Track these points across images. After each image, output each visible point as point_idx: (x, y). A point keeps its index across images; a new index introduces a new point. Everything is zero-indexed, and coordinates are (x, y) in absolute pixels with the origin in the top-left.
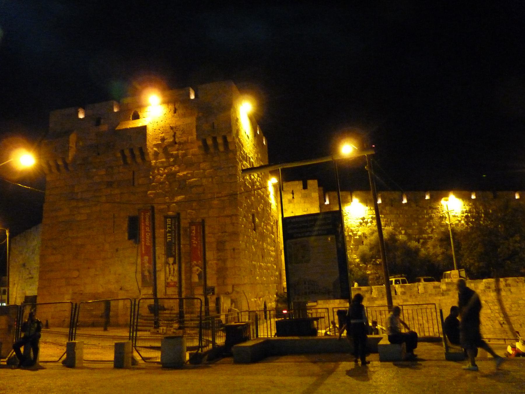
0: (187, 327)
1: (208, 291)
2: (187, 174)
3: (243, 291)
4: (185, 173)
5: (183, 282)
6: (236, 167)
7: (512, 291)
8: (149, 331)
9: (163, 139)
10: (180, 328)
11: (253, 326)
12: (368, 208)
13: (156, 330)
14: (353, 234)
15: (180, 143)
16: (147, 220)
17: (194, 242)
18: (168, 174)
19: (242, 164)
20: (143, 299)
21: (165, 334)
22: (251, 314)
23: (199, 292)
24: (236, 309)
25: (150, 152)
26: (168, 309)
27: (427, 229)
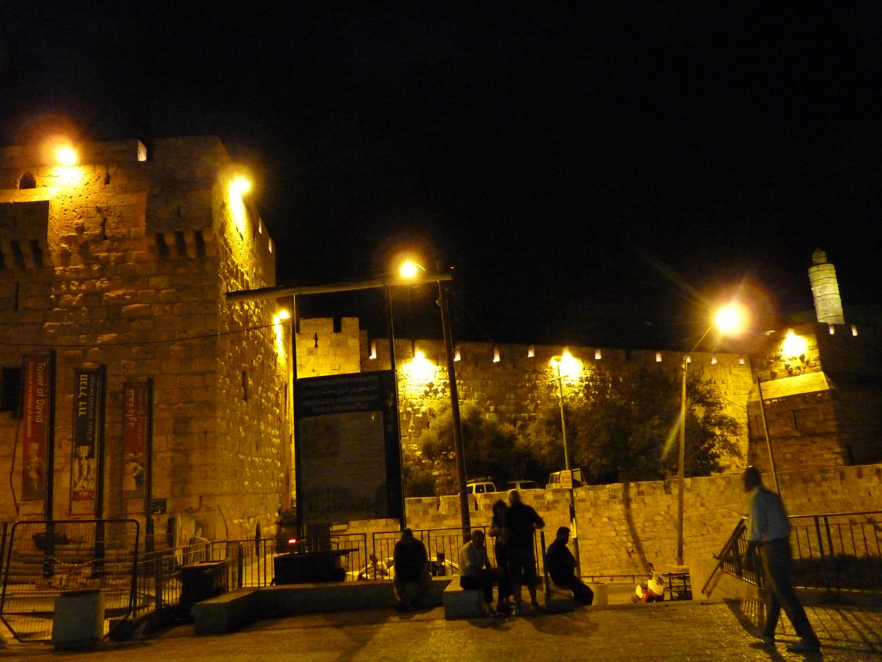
0: (110, 573)
1: (153, 506)
2: (124, 294)
3: (219, 506)
4: (120, 292)
5: (106, 490)
6: (215, 287)
7: (646, 501)
8: (33, 583)
9: (80, 229)
10: (94, 576)
11: (233, 566)
12: (439, 368)
13: (46, 582)
14: (413, 409)
15: (113, 239)
16: (40, 375)
17: (132, 419)
18: (86, 294)
19: (228, 284)
20: (20, 522)
21: (64, 588)
22: (231, 547)
23: (135, 509)
24: (203, 539)
25: (54, 251)
26: (74, 542)
27: (528, 405)
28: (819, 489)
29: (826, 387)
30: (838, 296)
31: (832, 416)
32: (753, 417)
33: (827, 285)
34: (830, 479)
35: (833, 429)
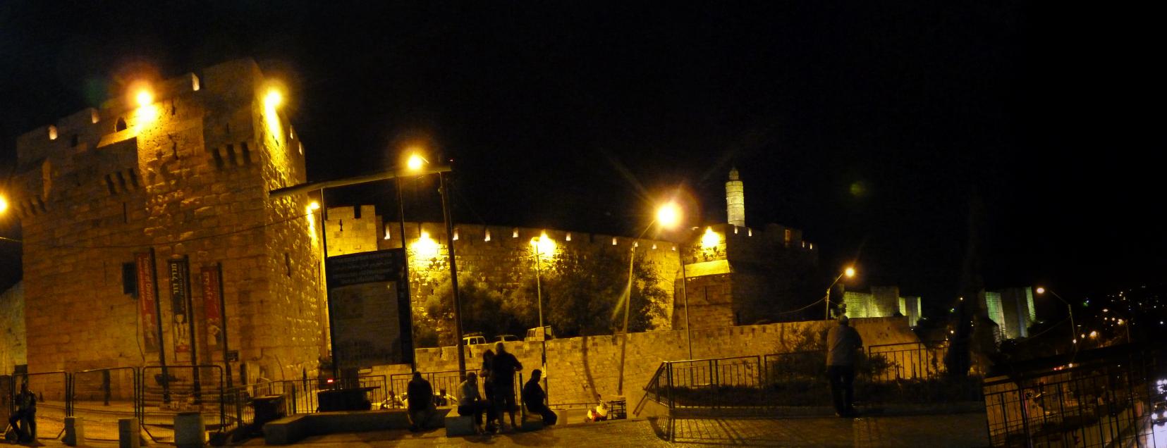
0: (205, 402)
1: (230, 356)
2: (195, 200)
3: (275, 356)
4: (192, 200)
5: (197, 345)
6: (260, 188)
8: (158, 406)
9: (160, 154)
10: (196, 403)
11: (289, 399)
13: (166, 406)
15: (183, 158)
16: (146, 267)
17: (209, 293)
18: (169, 204)
19: (270, 183)
20: (148, 367)
21: (178, 410)
22: (286, 385)
23: (218, 358)
24: (268, 379)
25: (144, 174)
26: (180, 380)
28: (716, 342)
29: (728, 271)
30: (743, 206)
31: (729, 291)
32: (678, 290)
33: (737, 197)
34: (724, 335)
35: (729, 301)
